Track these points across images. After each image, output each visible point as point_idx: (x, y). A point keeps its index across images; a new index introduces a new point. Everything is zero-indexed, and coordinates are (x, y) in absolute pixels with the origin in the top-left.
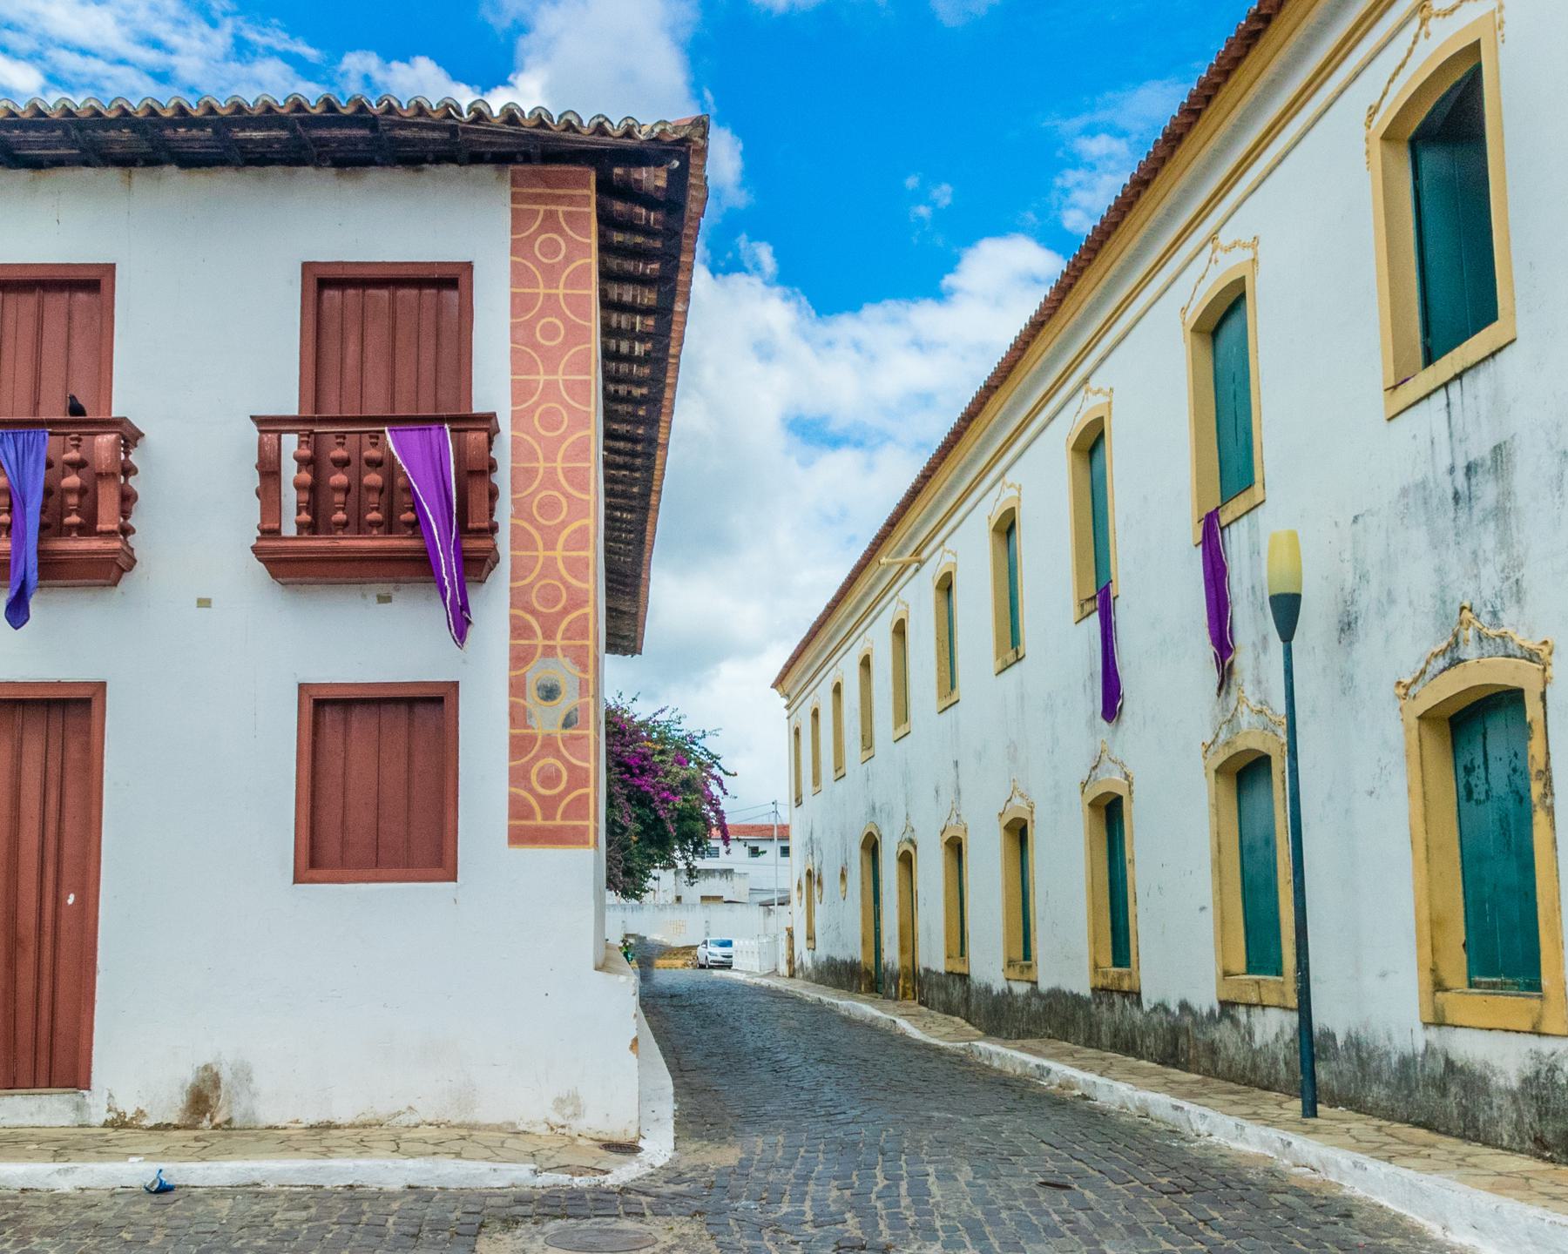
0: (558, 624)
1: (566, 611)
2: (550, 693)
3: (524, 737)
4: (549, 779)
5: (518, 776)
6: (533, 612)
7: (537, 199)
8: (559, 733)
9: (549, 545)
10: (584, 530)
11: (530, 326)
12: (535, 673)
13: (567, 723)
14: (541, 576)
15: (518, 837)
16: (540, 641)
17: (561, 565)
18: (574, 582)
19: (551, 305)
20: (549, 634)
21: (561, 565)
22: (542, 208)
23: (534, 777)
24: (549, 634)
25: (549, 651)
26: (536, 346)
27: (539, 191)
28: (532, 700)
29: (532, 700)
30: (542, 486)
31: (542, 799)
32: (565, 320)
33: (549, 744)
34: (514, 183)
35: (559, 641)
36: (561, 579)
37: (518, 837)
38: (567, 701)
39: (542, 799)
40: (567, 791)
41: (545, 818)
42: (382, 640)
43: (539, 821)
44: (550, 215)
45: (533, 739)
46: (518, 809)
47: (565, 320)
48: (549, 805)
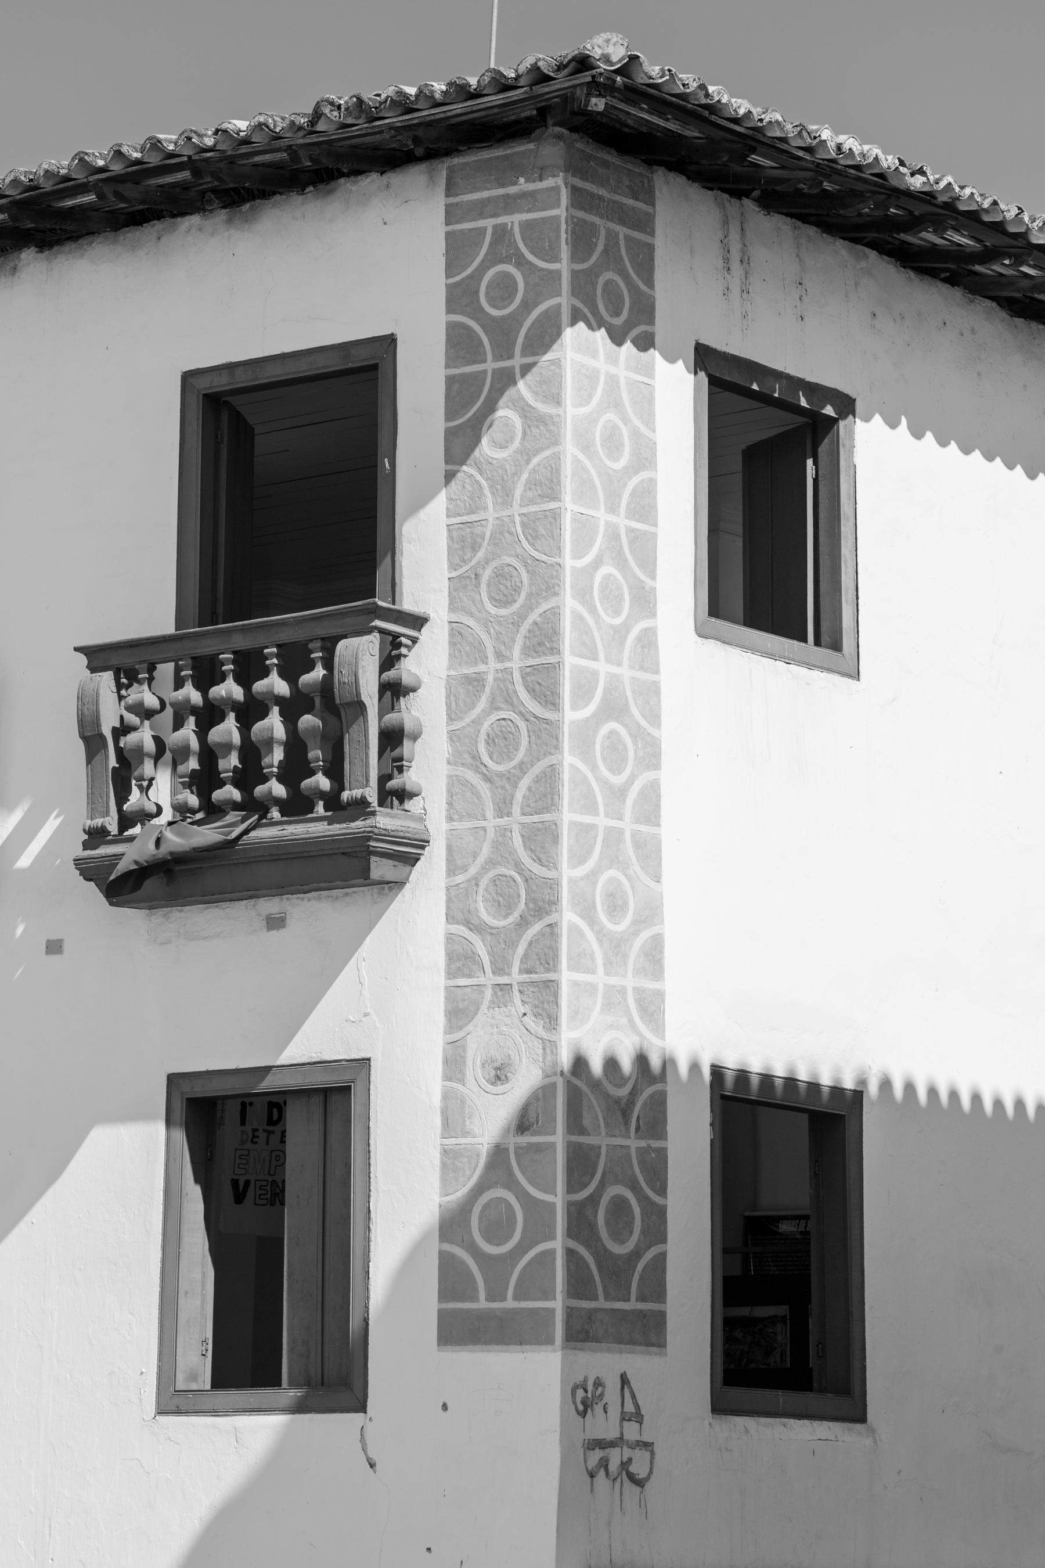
0: (513, 945)
1: (523, 923)
6: (479, 929)
7: (480, 210)
9: (503, 809)
14: (491, 863)
16: (489, 979)
21: (517, 841)
27: (485, 194)
28: (473, 1084)
29: (473, 1084)
30: (493, 707)
34: (450, 190)
35: (516, 976)
36: (518, 866)
41: (490, 1298)
43: (482, 1303)
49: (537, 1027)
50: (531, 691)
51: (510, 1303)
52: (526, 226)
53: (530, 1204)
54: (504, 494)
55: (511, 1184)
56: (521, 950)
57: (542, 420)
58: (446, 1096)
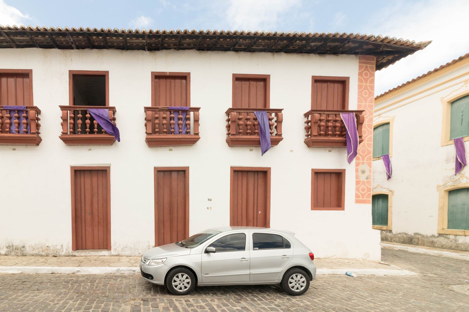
1: (367, 155)
2: (363, 172)
3: (358, 181)
4: (363, 190)
5: (357, 189)
8: (365, 180)
10: (371, 137)
11: (362, 91)
12: (361, 167)
13: (367, 179)
15: (357, 202)
16: (361, 161)
17: (366, 145)
18: (369, 149)
19: (366, 88)
20: (363, 160)
21: (366, 145)
22: (365, 65)
23: (360, 189)
24: (363, 160)
25: (363, 163)
26: (363, 97)
29: (360, 173)
31: (362, 194)
32: (369, 91)
33: (363, 182)
35: (365, 161)
37: (357, 202)
38: (367, 174)
39: (362, 194)
40: (366, 193)
42: (329, 160)
43: (361, 198)
44: (366, 67)
45: (360, 182)
46: (357, 196)
47: (369, 91)
48: (363, 195)
49: (368, 167)
50: (368, 127)
51: (365, 199)
52: (370, 67)
53: (368, 188)
54: (366, 102)
55: (365, 185)
56: (366, 158)
57: (371, 93)
58: (356, 174)
